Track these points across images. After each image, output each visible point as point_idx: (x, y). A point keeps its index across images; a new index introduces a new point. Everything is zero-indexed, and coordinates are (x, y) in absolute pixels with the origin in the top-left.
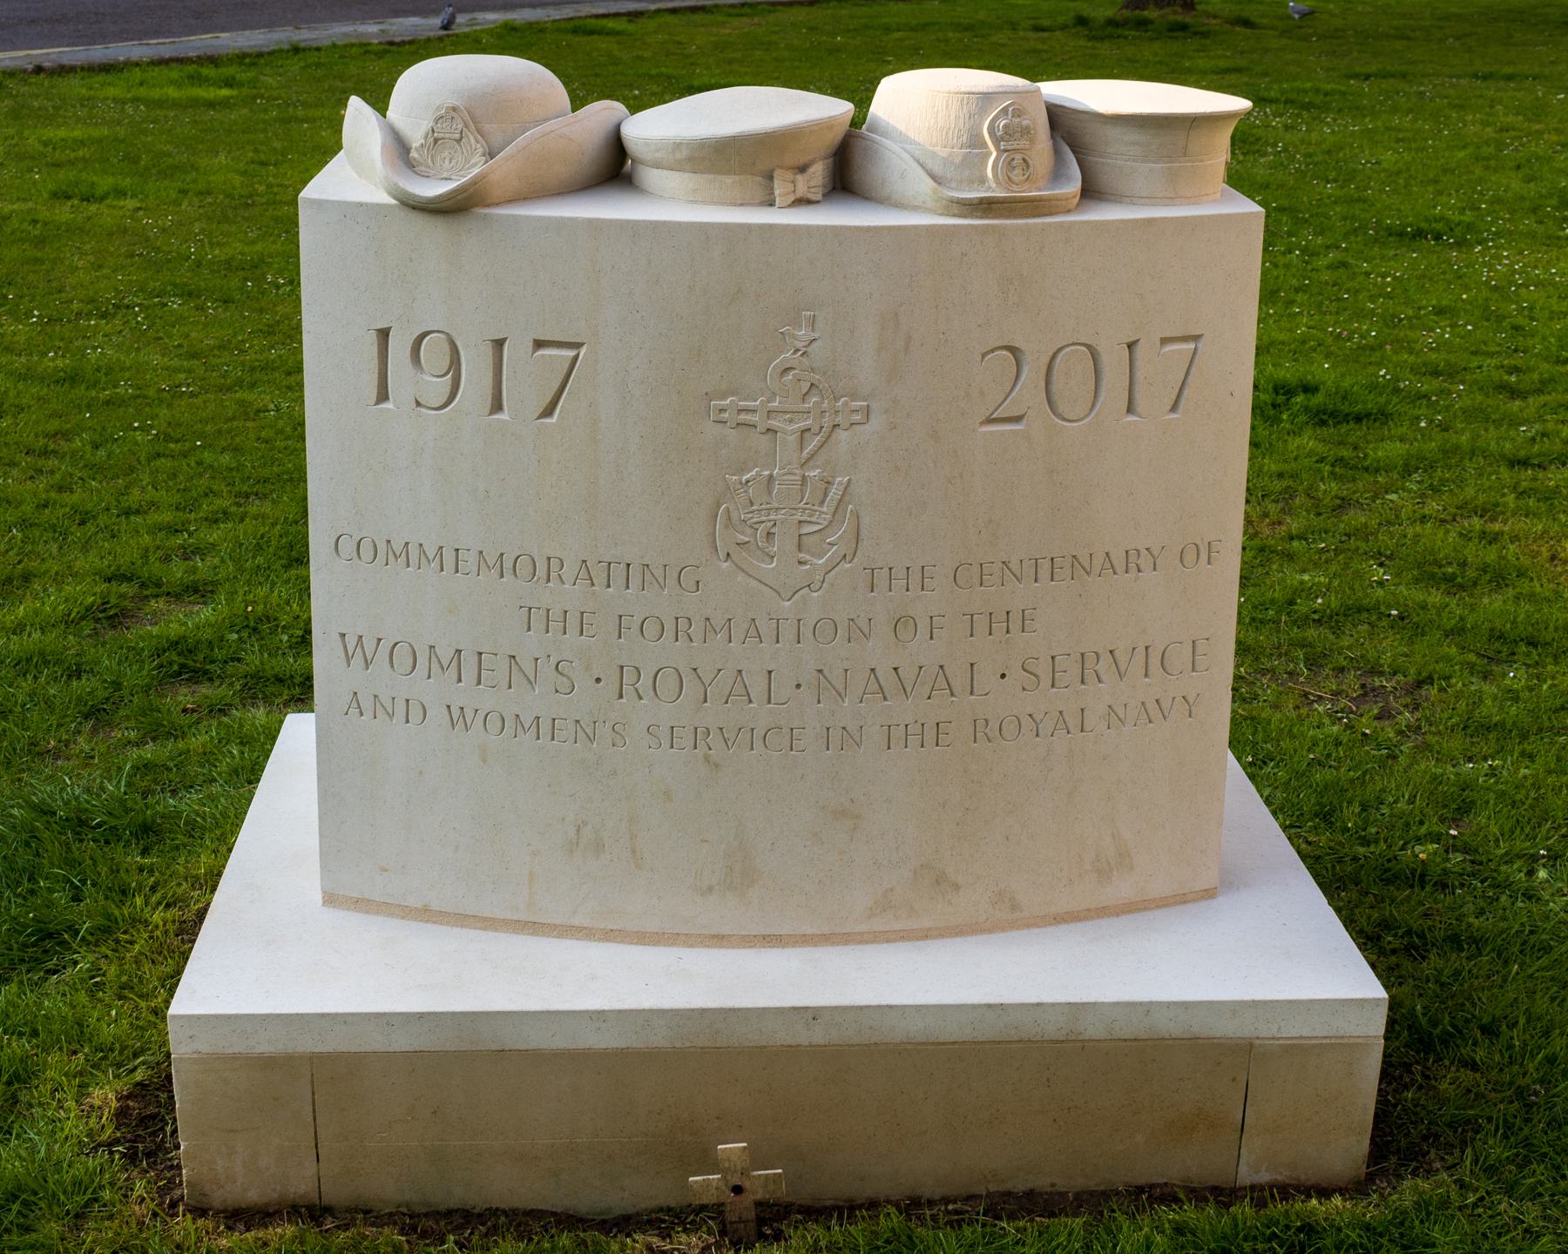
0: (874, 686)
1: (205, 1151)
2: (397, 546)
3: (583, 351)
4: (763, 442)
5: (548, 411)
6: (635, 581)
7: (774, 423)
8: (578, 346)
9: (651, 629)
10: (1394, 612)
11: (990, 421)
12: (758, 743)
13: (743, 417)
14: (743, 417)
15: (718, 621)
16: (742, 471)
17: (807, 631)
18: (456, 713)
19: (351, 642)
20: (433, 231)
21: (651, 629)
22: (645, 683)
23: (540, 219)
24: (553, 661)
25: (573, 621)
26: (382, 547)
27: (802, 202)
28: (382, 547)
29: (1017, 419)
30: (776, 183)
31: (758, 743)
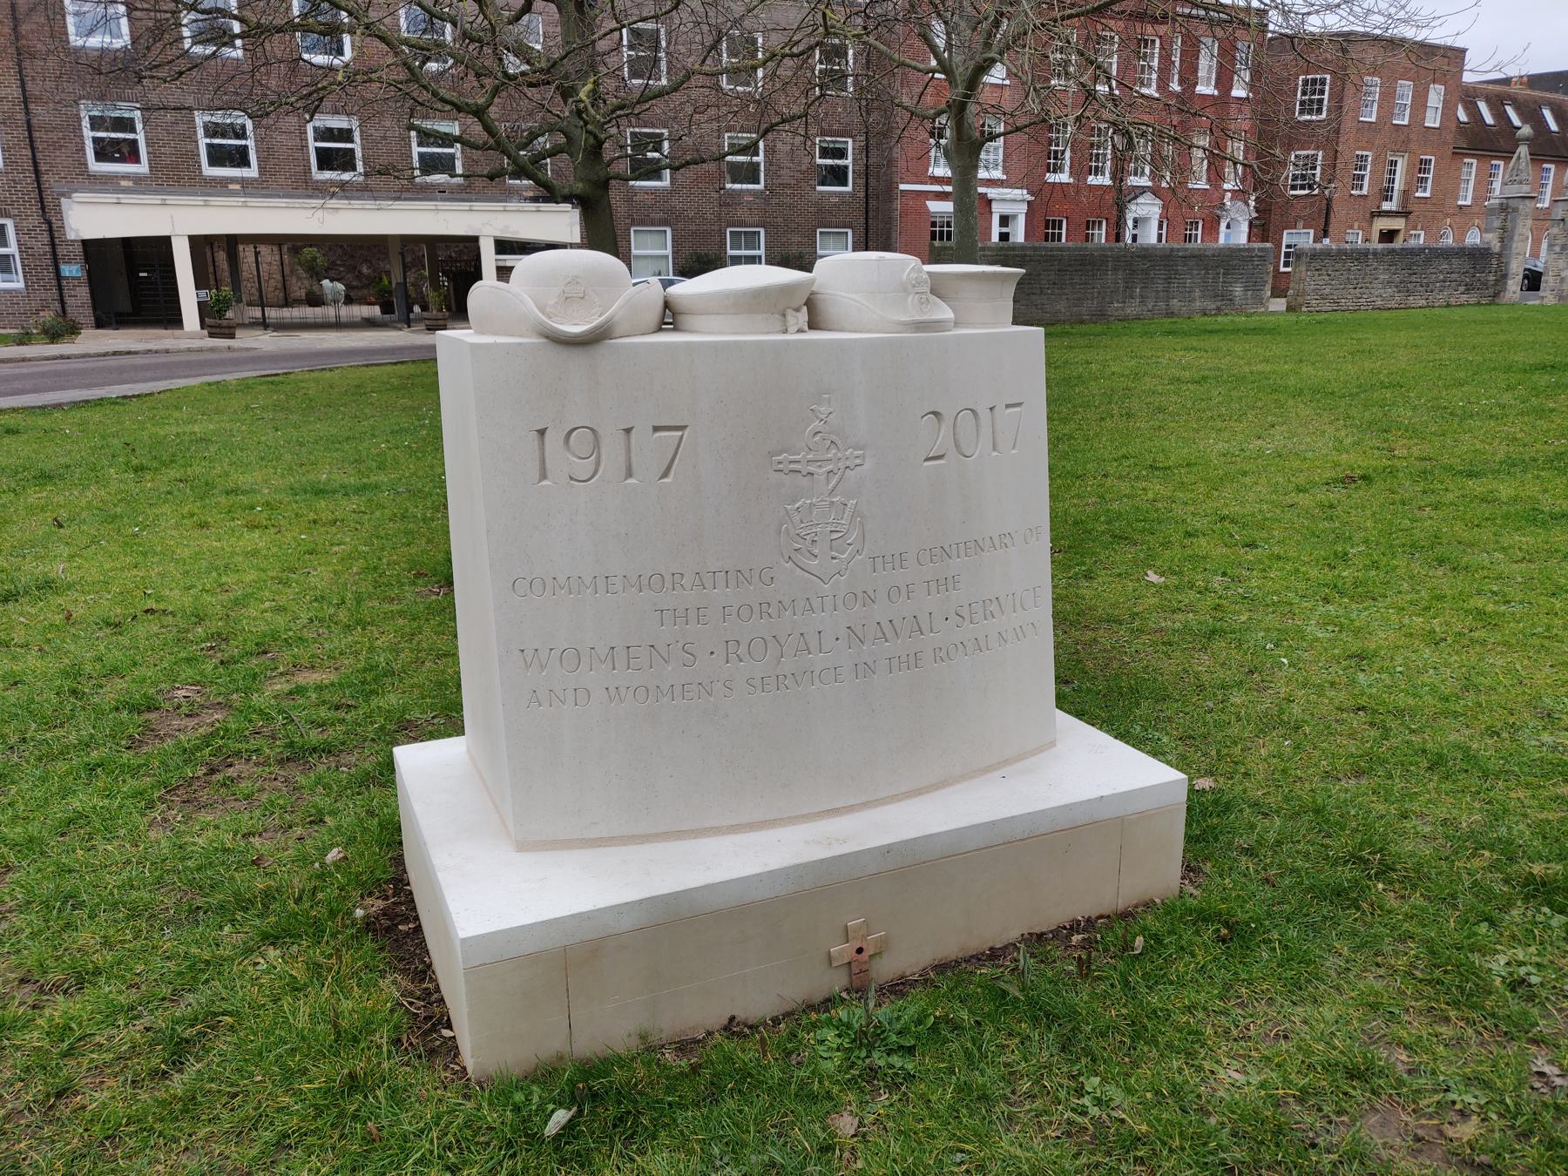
0: (880, 635)
1: (477, 1041)
2: (562, 579)
3: (687, 432)
4: (805, 482)
5: (665, 474)
6: (732, 583)
7: (811, 469)
8: (682, 428)
9: (745, 612)
10: (1153, 577)
11: (928, 459)
12: (816, 681)
13: (792, 466)
14: (792, 466)
15: (786, 602)
16: (794, 502)
17: (840, 603)
18: (612, 691)
19: (529, 653)
20: (576, 360)
21: (745, 612)
22: (742, 650)
23: (652, 344)
24: (680, 645)
25: (692, 614)
26: (549, 581)
27: (800, 331)
28: (549, 581)
29: (1019, 405)
30: (789, 317)
31: (816, 681)
